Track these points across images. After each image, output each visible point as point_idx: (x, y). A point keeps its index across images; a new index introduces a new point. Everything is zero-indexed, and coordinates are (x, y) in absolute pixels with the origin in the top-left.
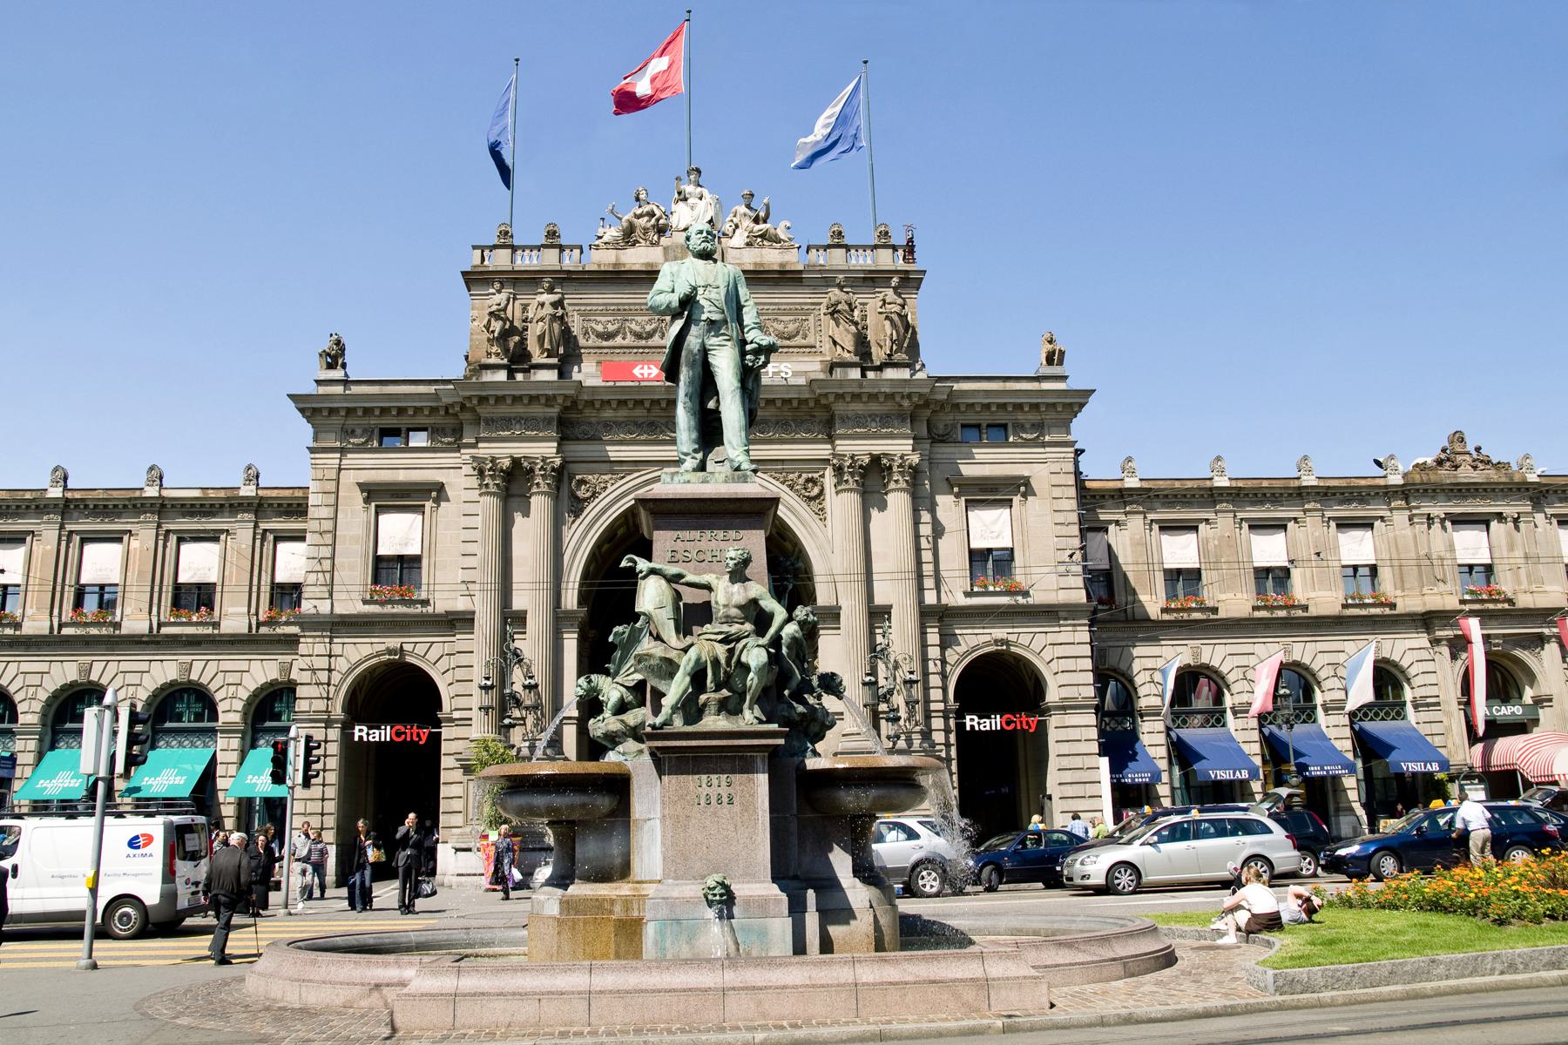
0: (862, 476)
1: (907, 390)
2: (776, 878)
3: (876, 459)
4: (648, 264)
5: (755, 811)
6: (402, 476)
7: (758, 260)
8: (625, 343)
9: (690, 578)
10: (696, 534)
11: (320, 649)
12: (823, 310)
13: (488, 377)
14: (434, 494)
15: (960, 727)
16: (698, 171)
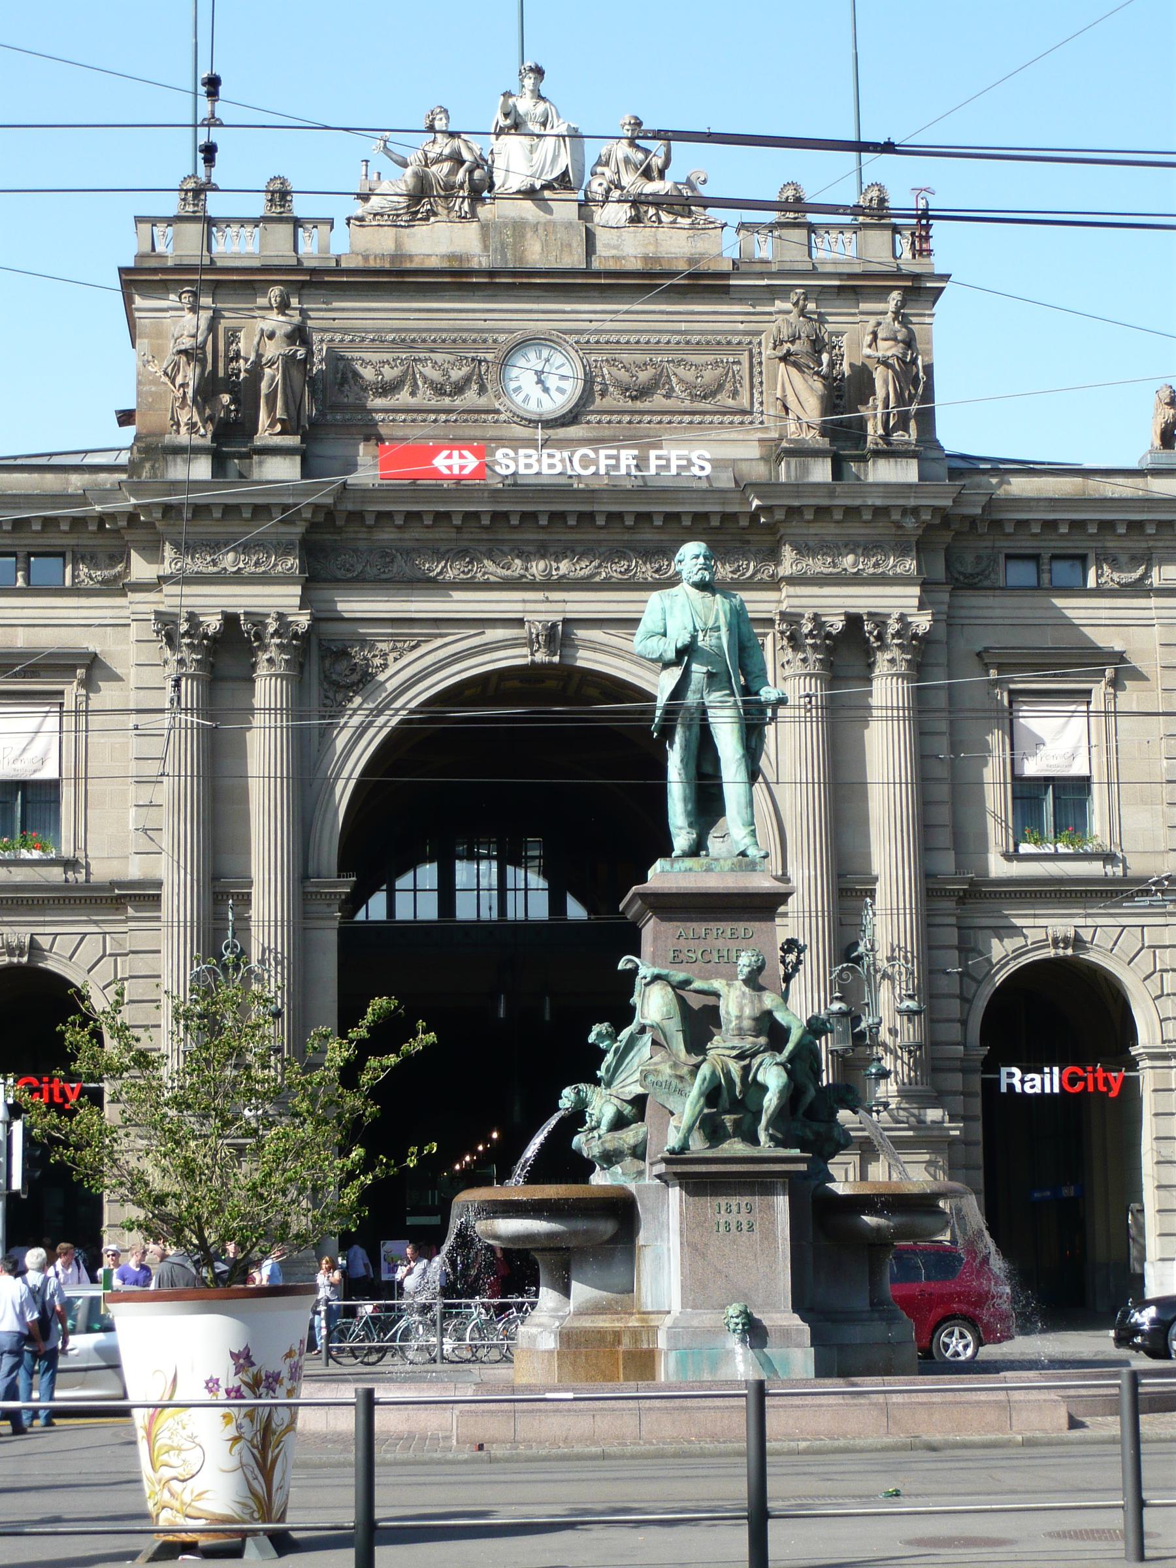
0: (830, 651)
1: (912, 502)
2: (796, 1308)
3: (854, 621)
4: (452, 257)
5: (775, 1239)
7: (650, 251)
8: (412, 401)
9: (697, 984)
10: (700, 928)
12: (767, 352)
13: (177, 471)
14: (80, 672)
15: (991, 1086)
16: (539, 72)
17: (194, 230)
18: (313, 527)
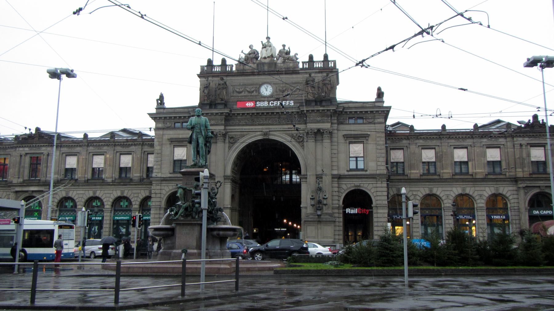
3: (319, 130)
6: (181, 136)
11: (159, 187)
15: (344, 212)
17: (209, 67)
18: (226, 116)
